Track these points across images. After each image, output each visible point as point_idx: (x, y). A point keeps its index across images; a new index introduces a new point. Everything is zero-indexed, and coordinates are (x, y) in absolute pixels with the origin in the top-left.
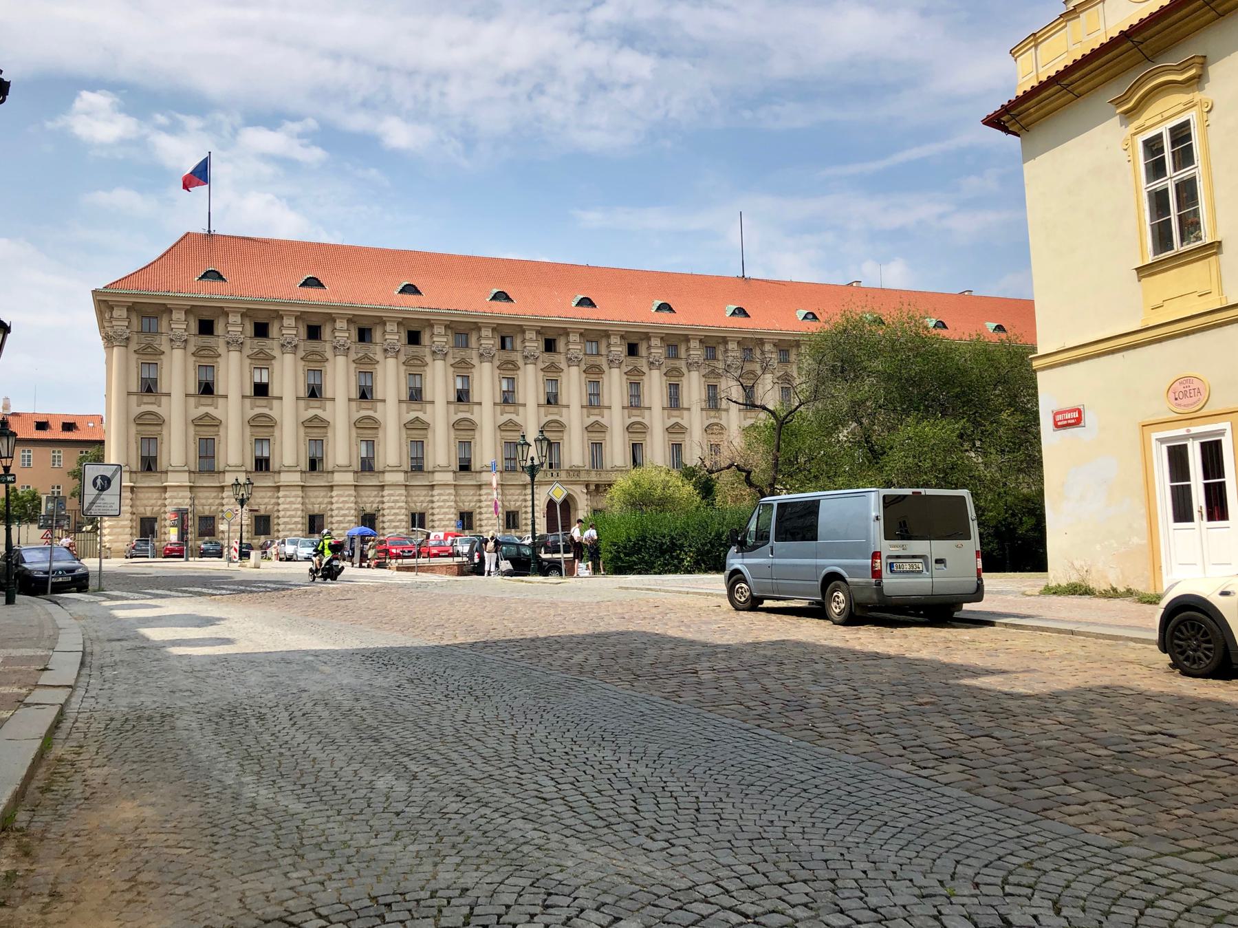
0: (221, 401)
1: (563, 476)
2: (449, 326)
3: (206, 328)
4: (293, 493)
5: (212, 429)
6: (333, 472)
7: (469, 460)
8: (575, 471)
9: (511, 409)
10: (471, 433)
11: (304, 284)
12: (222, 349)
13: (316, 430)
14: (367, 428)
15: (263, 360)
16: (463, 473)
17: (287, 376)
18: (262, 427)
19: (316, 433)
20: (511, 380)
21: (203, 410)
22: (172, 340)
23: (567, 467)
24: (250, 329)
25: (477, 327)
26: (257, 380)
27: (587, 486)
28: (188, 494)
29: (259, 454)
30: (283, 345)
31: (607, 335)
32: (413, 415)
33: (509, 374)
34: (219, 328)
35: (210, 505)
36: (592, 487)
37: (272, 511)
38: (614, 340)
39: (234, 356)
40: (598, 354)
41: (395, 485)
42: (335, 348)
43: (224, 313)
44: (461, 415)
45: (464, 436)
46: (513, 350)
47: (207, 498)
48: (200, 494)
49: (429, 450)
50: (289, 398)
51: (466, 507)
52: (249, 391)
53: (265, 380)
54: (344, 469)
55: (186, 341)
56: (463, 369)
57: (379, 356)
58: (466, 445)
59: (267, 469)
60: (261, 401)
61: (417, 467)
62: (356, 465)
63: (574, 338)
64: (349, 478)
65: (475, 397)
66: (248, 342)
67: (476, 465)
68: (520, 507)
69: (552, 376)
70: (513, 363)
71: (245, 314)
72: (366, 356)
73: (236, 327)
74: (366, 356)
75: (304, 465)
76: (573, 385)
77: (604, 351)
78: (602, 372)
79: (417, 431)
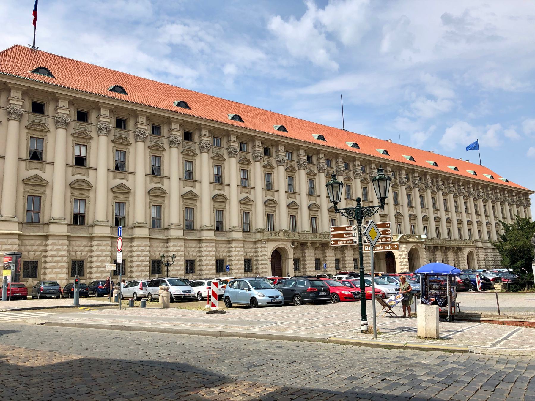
0: (48, 167)
1: (282, 236)
2: (212, 131)
3: (38, 108)
4: (105, 243)
5: (39, 188)
6: (133, 228)
7: (222, 223)
8: (286, 233)
9: (246, 190)
10: (223, 204)
11: (113, 90)
12: (51, 126)
13: (122, 195)
14: (157, 196)
15: (82, 139)
16: (218, 232)
17: (101, 152)
18: (80, 190)
19: (121, 198)
20: (246, 171)
21: (32, 173)
22: (9, 113)
23: (278, 230)
24: (74, 115)
25: (228, 134)
26: (77, 153)
27: (293, 243)
28: (16, 241)
29: (77, 211)
30: (100, 129)
31: (298, 148)
32: (188, 189)
33: (245, 168)
34: (50, 109)
35: (35, 251)
36: (296, 244)
37: (86, 257)
38: (302, 152)
39: (61, 132)
40: (292, 160)
41: (177, 239)
42: (138, 136)
43: (54, 98)
44: (217, 192)
45: (219, 206)
46: (247, 152)
47: (33, 245)
48: (26, 242)
49: (197, 214)
50: (102, 171)
51: (221, 256)
52: (71, 161)
53: (83, 154)
54: (142, 225)
55: (21, 115)
56: (218, 162)
57: (166, 146)
58: (220, 212)
59: (82, 223)
60: (80, 170)
61: (189, 226)
62: (149, 223)
63: (281, 148)
64: (145, 232)
65: (226, 181)
66: (72, 124)
67: (226, 226)
68: (252, 256)
69: (269, 171)
70: (248, 160)
71: (72, 102)
72: (157, 145)
73: (64, 110)
74: (157, 145)
75: (112, 221)
76: (280, 176)
77: (295, 159)
78: (294, 171)
79: (190, 200)
